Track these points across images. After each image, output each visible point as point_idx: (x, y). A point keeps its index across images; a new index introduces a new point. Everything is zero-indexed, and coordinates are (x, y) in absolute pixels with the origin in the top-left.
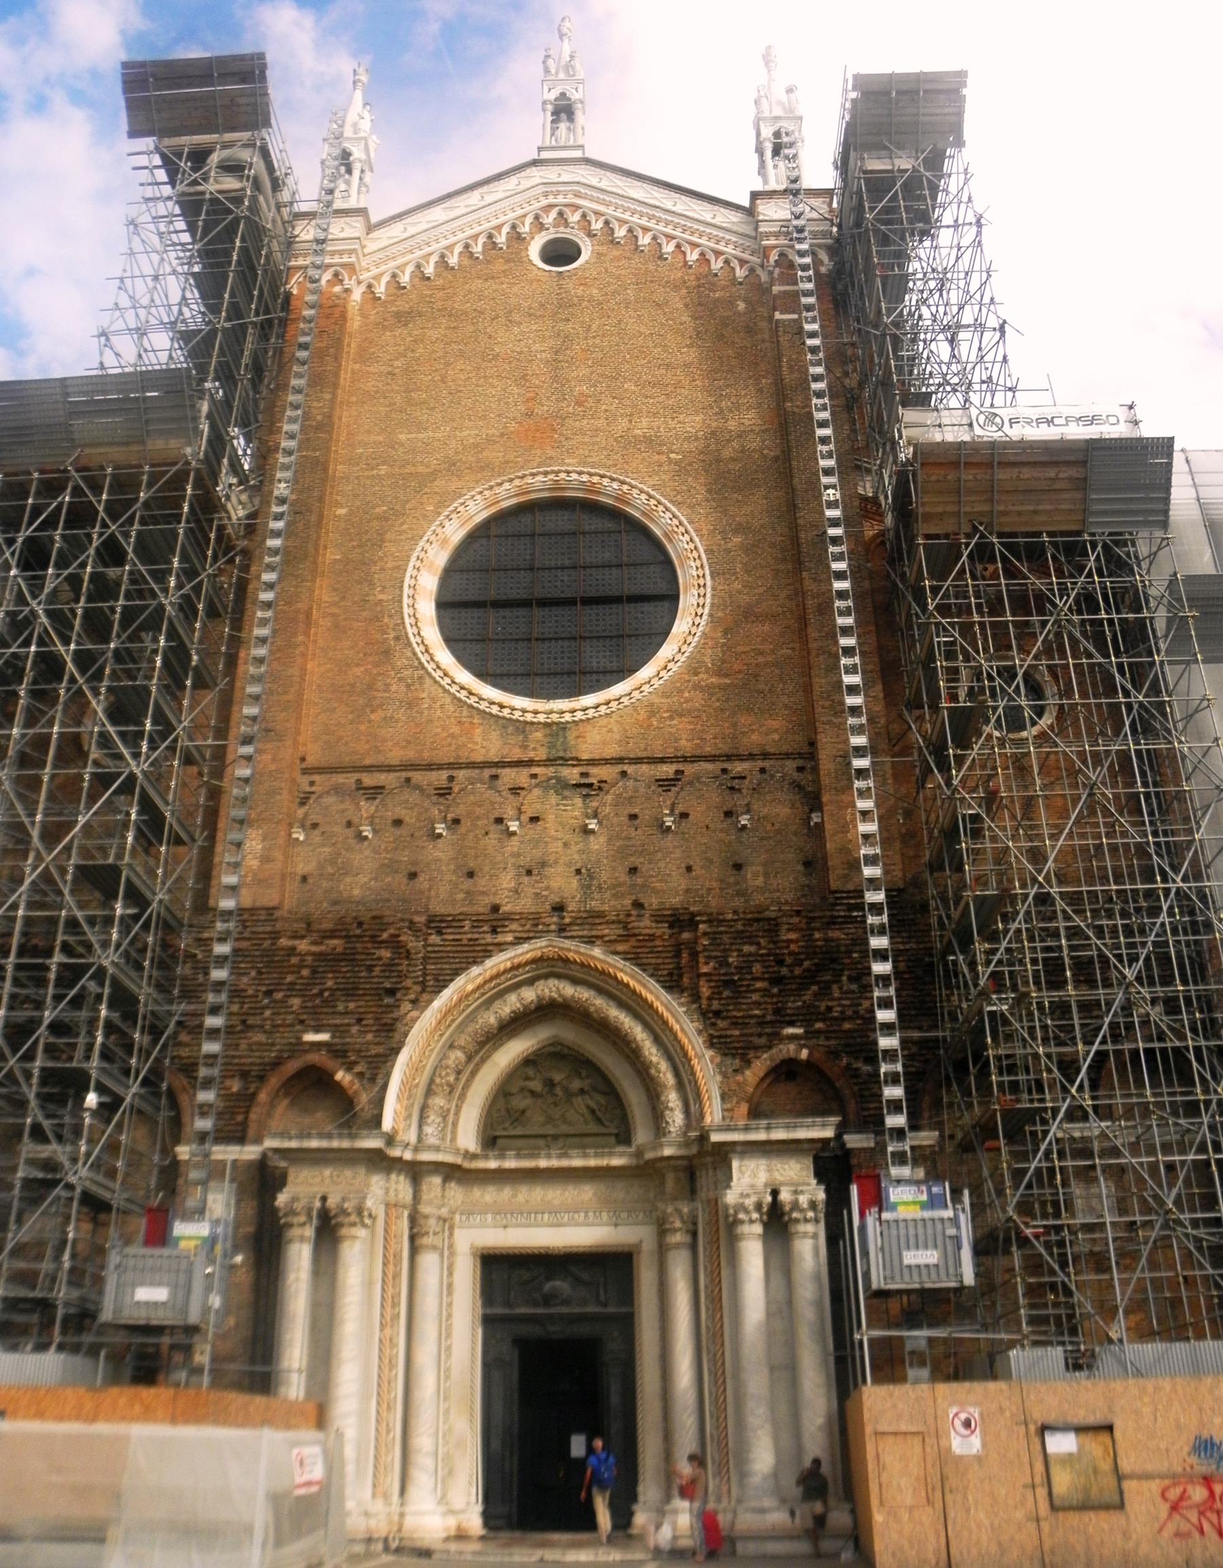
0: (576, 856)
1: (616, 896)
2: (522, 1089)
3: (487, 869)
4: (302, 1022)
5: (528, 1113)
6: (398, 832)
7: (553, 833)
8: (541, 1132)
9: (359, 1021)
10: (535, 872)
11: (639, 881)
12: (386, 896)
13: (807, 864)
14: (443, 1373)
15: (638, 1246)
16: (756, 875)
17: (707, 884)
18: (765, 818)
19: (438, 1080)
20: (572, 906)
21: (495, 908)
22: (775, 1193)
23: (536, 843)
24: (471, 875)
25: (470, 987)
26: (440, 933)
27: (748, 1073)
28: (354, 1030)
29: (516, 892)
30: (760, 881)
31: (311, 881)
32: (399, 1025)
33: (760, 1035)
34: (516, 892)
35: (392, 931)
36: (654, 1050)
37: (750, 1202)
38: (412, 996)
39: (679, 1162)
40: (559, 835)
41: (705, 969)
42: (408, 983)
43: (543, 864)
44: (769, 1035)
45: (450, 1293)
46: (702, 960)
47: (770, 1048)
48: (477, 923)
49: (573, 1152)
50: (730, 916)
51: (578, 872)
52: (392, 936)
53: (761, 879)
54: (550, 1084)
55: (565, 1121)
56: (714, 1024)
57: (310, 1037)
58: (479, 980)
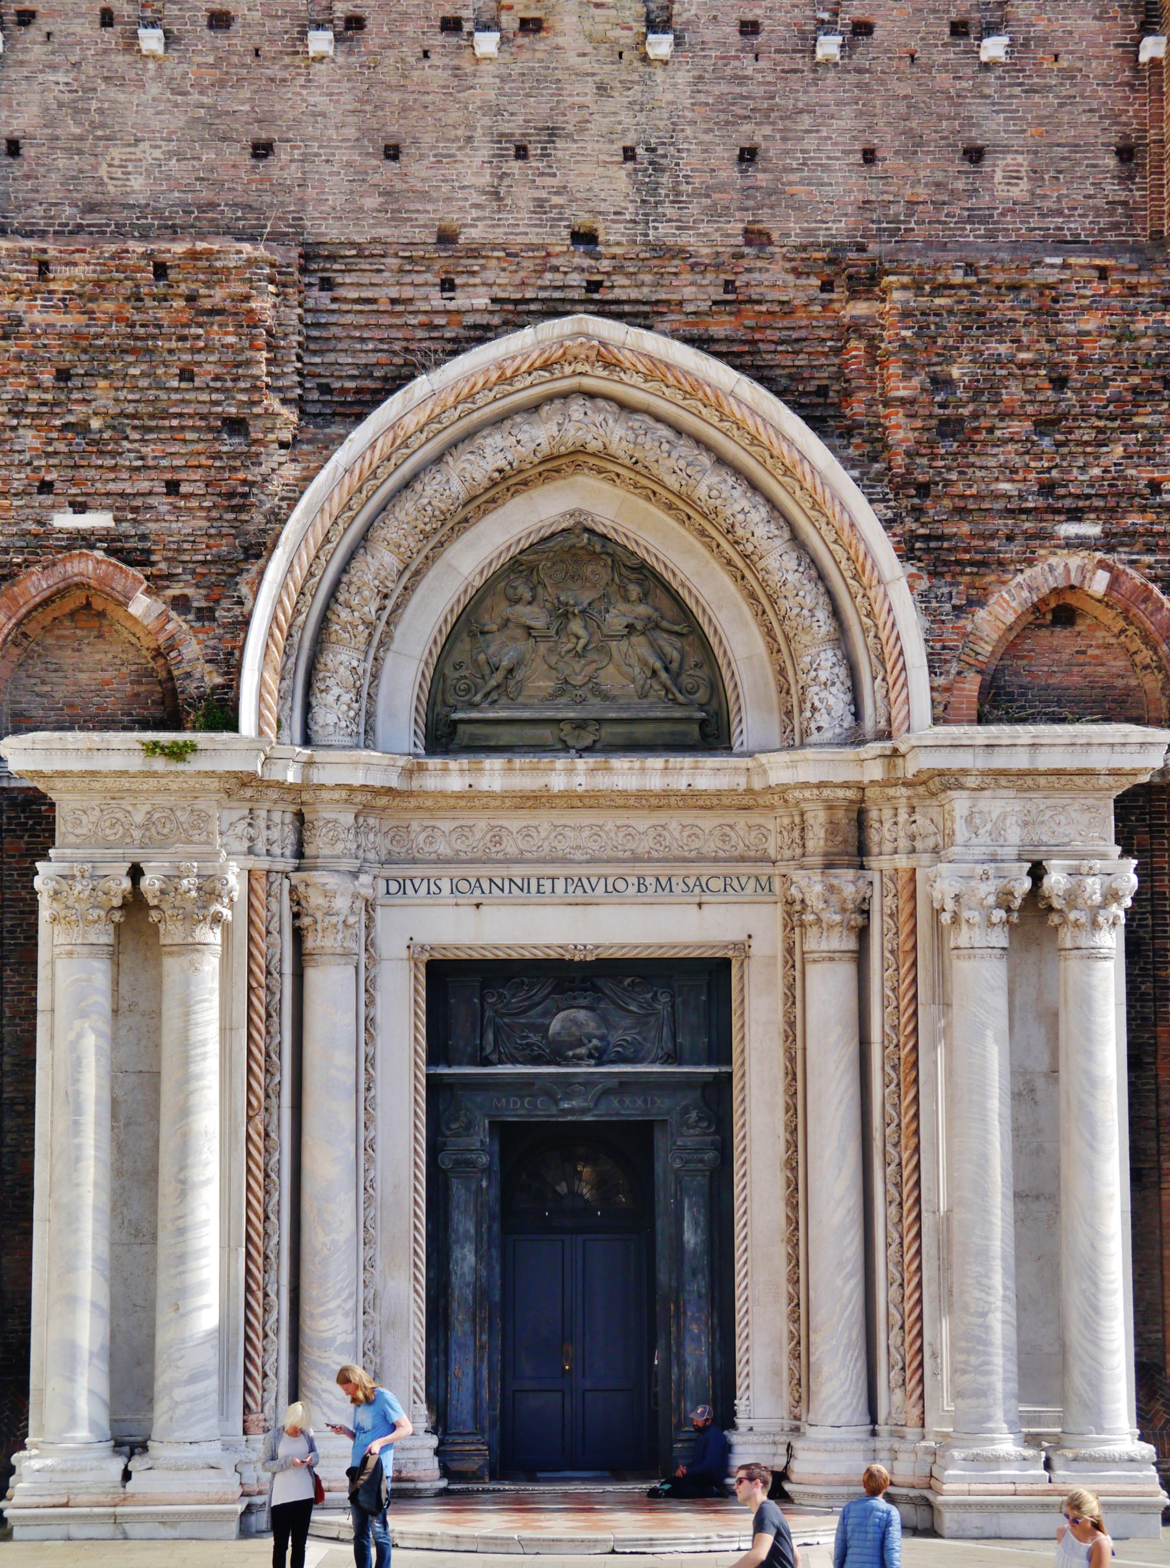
0: (626, 118)
1: (715, 213)
2: (506, 623)
3: (428, 139)
4: (46, 487)
5: (519, 674)
6: (220, 39)
7: (573, 60)
8: (549, 714)
9: (172, 487)
10: (534, 150)
11: (762, 179)
12: (206, 195)
13: (1125, 153)
14: (366, 1190)
15: (743, 948)
16: (1013, 177)
17: (908, 192)
18: (1042, 40)
19: (344, 614)
20: (613, 235)
22: (1037, 872)
23: (538, 81)
24: (392, 153)
25: (411, 423)
26: (327, 284)
27: (981, 614)
28: (162, 504)
29: (496, 195)
30: (1020, 191)
31: (28, 151)
33: (1010, 538)
34: (496, 195)
36: (790, 562)
37: (987, 891)
39: (840, 793)
40: (585, 65)
43: (553, 133)
44: (1029, 537)
45: (370, 1039)
46: (895, 369)
47: (1030, 562)
48: (413, 261)
49: (620, 763)
50: (958, 277)
51: (629, 154)
53: (1024, 185)
54: (562, 614)
56: (917, 512)
57: (66, 520)
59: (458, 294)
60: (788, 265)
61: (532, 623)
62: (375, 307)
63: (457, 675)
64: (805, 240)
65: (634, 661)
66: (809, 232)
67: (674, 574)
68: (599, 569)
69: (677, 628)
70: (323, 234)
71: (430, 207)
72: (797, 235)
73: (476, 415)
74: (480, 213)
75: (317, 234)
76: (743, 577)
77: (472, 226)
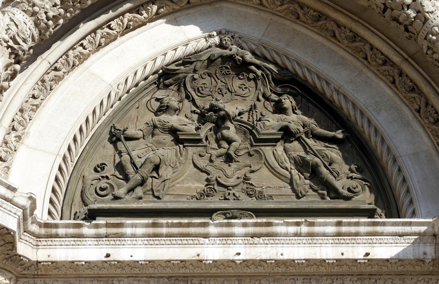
63: (98, 175)
65: (288, 165)
67: (328, 83)
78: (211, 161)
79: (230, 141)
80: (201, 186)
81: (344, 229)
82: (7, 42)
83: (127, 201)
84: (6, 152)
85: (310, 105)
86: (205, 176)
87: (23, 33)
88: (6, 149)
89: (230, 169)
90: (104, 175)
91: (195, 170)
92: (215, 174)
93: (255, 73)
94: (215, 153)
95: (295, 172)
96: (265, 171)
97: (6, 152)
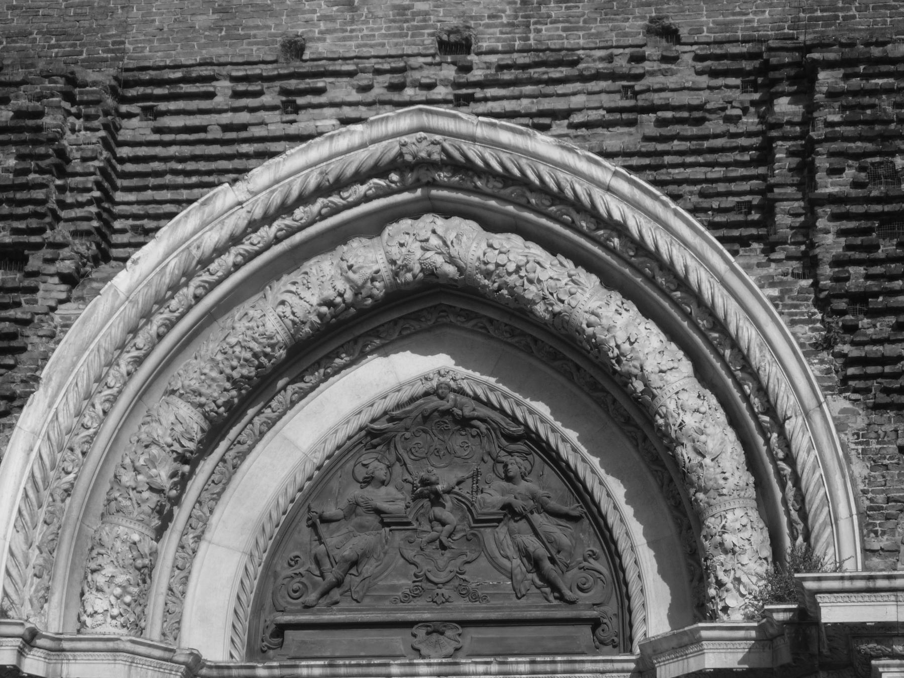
5: (368, 568)
12: (17, 23)
19: (127, 478)
21: (295, 48)
26: (151, 113)
32: (34, 341)
35: (23, 103)
38: (67, 266)
41: (828, 186)
42: (62, 232)
46: (822, 162)
52: (19, 114)
55: (464, 592)
58: (237, 221)
59: (303, 115)
60: (699, 66)
61: (385, 506)
62: (202, 136)
63: (290, 572)
64: (720, 36)
65: (511, 551)
66: (725, 26)
68: (473, 443)
69: (565, 509)
70: (146, 58)
71: (271, 22)
72: (710, 30)
73: (298, 237)
74: (330, 25)
75: (139, 59)
76: (645, 438)
77: (319, 39)
78: (422, 549)
79: (443, 524)
80: (406, 583)
81: (539, 667)
82: (170, 446)
83: (321, 611)
84: (183, 558)
85: (546, 467)
86: (413, 570)
87: (189, 433)
88: (183, 554)
89: (442, 559)
90: (297, 572)
91: (402, 560)
92: (426, 567)
93: (478, 428)
94: (426, 537)
95: (517, 562)
96: (483, 562)
97: (183, 558)
